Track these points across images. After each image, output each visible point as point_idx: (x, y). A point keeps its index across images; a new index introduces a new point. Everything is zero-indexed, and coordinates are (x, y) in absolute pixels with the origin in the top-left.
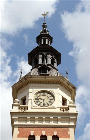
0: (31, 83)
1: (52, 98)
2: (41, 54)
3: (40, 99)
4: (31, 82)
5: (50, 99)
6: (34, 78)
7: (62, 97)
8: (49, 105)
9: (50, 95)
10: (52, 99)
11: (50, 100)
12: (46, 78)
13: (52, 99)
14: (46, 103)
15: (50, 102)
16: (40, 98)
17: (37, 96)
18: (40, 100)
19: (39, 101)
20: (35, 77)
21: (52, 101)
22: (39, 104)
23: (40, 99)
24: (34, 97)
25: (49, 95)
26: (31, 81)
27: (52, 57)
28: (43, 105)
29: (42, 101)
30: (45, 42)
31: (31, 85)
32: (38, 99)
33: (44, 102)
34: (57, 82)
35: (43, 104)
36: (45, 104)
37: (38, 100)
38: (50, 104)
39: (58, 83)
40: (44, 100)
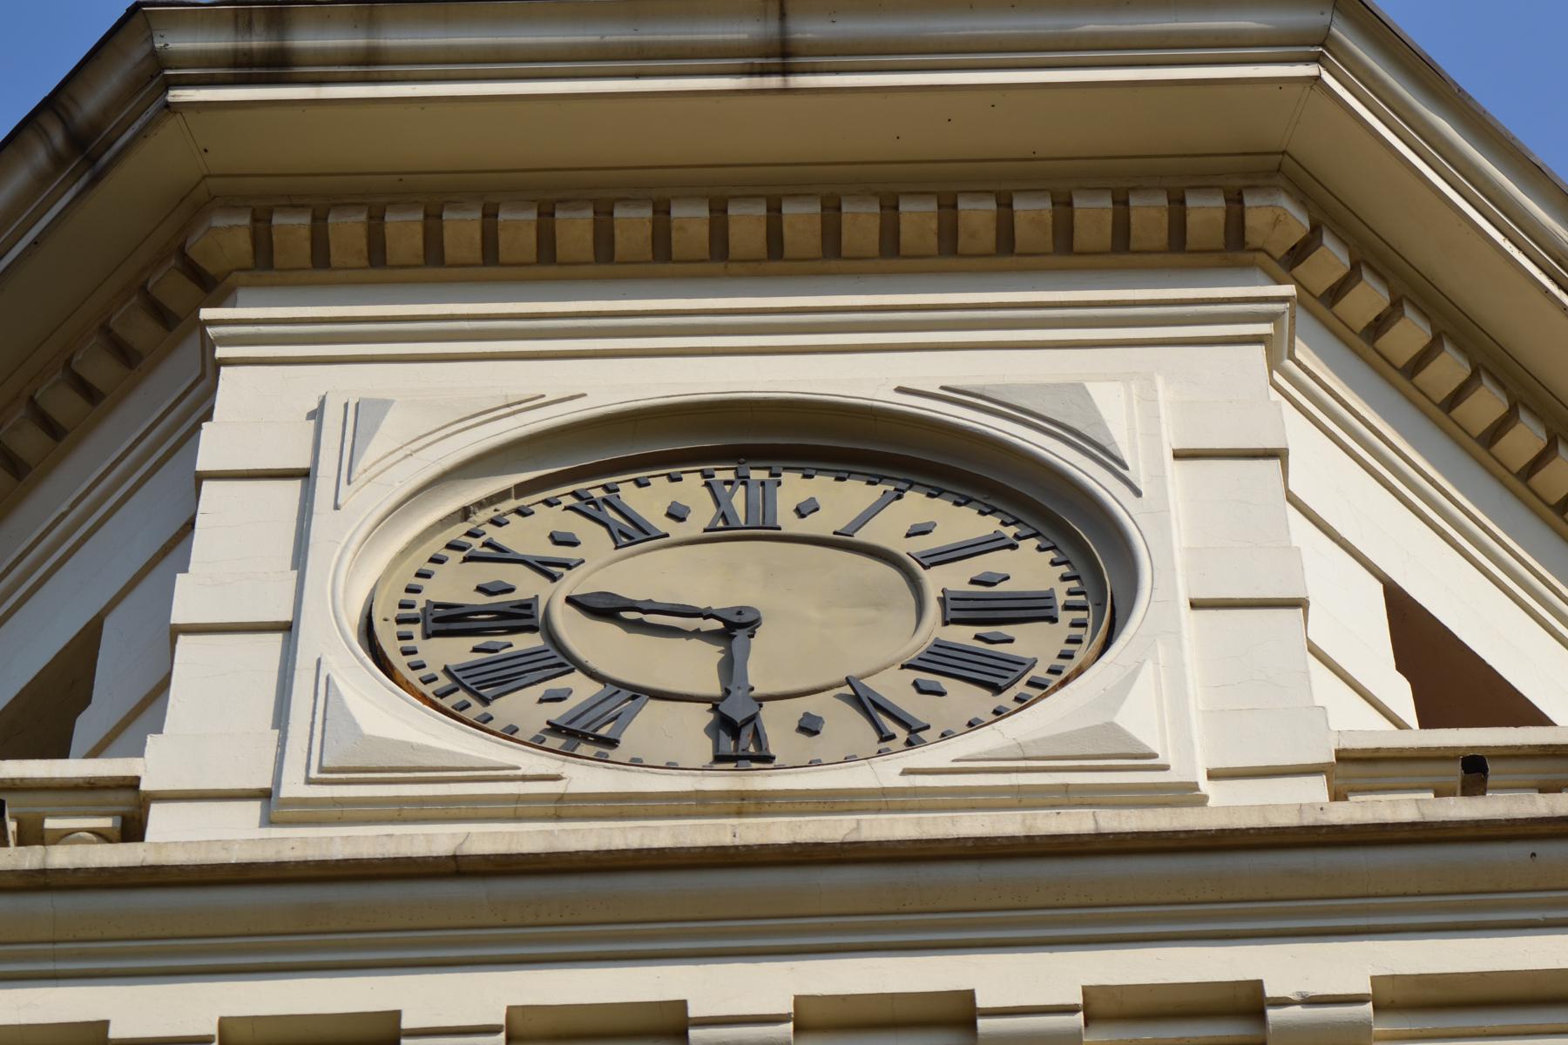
1: (1029, 568)
3: (603, 609)
5: (958, 610)
7: (1404, 612)
9: (961, 522)
10: (1036, 609)
11: (963, 635)
13: (1036, 609)
15: (938, 663)
16: (573, 583)
17: (499, 555)
18: (578, 633)
19: (564, 661)
21: (1033, 643)
22: (556, 712)
23: (603, 609)
24: (356, 568)
25: (916, 505)
28: (704, 749)
29: (692, 665)
32: (521, 616)
33: (729, 668)
35: (701, 716)
36: (777, 725)
38: (963, 698)
40: (734, 628)
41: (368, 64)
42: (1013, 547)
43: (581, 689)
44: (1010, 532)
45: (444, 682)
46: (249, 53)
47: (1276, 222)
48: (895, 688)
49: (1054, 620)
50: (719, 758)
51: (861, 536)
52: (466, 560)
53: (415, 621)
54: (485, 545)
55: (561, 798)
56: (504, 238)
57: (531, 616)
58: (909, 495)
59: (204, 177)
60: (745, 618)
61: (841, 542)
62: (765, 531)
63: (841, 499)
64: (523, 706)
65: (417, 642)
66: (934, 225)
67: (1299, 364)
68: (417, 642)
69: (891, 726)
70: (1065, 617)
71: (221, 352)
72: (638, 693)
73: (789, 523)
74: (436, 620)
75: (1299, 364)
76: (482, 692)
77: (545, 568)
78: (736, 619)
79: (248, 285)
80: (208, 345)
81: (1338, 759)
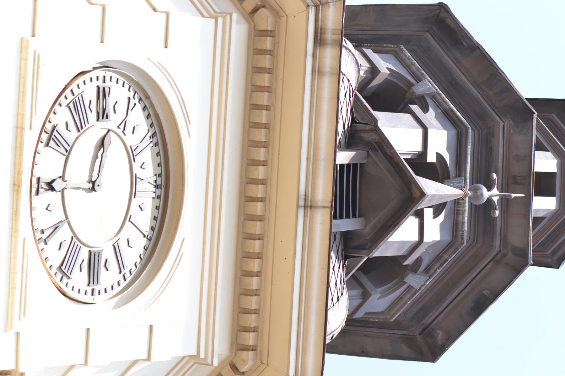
0: (257, 34)
2: (458, 147)
4: (267, 44)
6: (317, 72)
8: (43, 238)
9: (132, 256)
11: (84, 255)
12: (309, 206)
14: (58, 215)
20: (327, 83)
22: (61, 128)
26: (271, 33)
27: (419, 261)
29: (78, 172)
30: (544, 184)
31: (238, 29)
32: (102, 115)
34: (250, 339)
37: (92, 116)
39: (238, 347)
41: (318, 72)
42: (120, 272)
43: (71, 136)
44: (127, 271)
45: (76, 92)
46: (324, 33)
47: (243, 361)
48: (64, 234)
49: (88, 285)
50: (39, 179)
51: (127, 223)
52: (129, 98)
53: (104, 82)
54: (135, 104)
55: (23, 128)
56: (257, 112)
57: (103, 118)
58: (145, 239)
59: (287, 16)
60: (96, 187)
61: (127, 217)
62: (133, 193)
63: (144, 219)
64: (62, 116)
65: (95, 83)
66: (251, 251)
67: (193, 365)
68: (95, 83)
69: (47, 233)
70: (89, 289)
71: (220, 20)
72: (69, 152)
73: (135, 202)
74: (104, 88)
75: (193, 365)
76: (72, 104)
77: (124, 123)
78: (96, 184)
79: (249, 27)
80: (223, 14)
81: (22, 373)
